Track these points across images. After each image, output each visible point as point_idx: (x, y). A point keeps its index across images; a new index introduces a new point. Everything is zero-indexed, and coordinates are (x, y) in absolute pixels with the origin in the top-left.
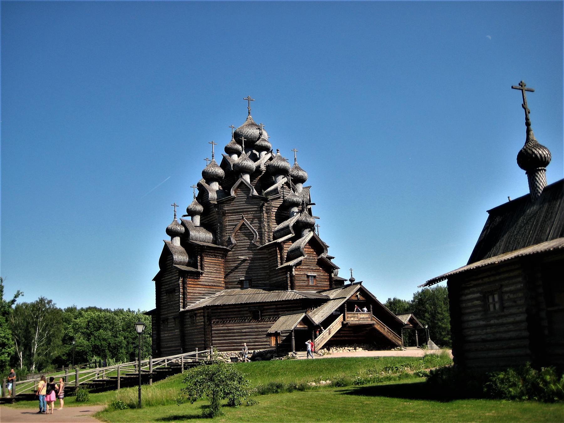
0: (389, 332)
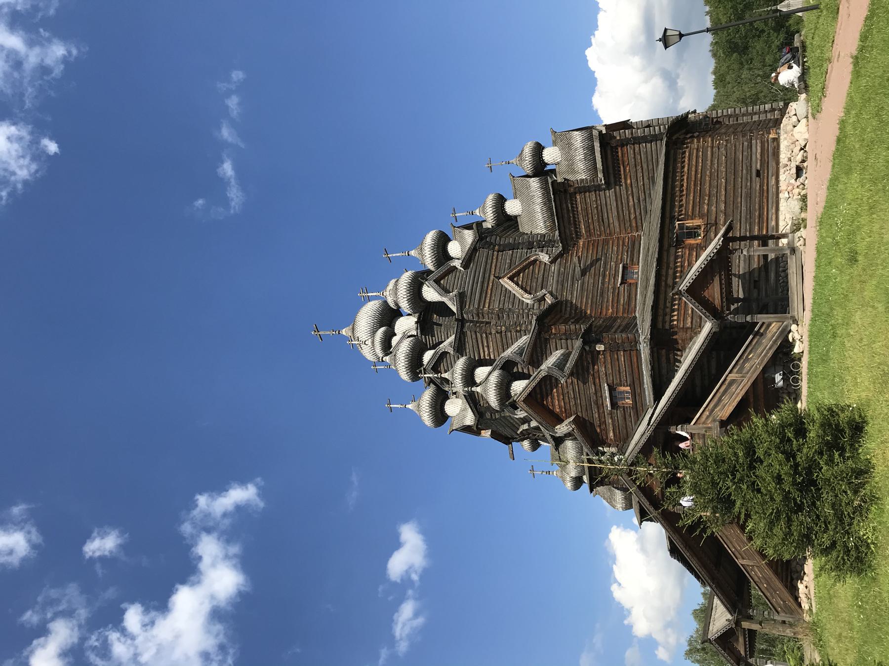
0: (742, 367)
